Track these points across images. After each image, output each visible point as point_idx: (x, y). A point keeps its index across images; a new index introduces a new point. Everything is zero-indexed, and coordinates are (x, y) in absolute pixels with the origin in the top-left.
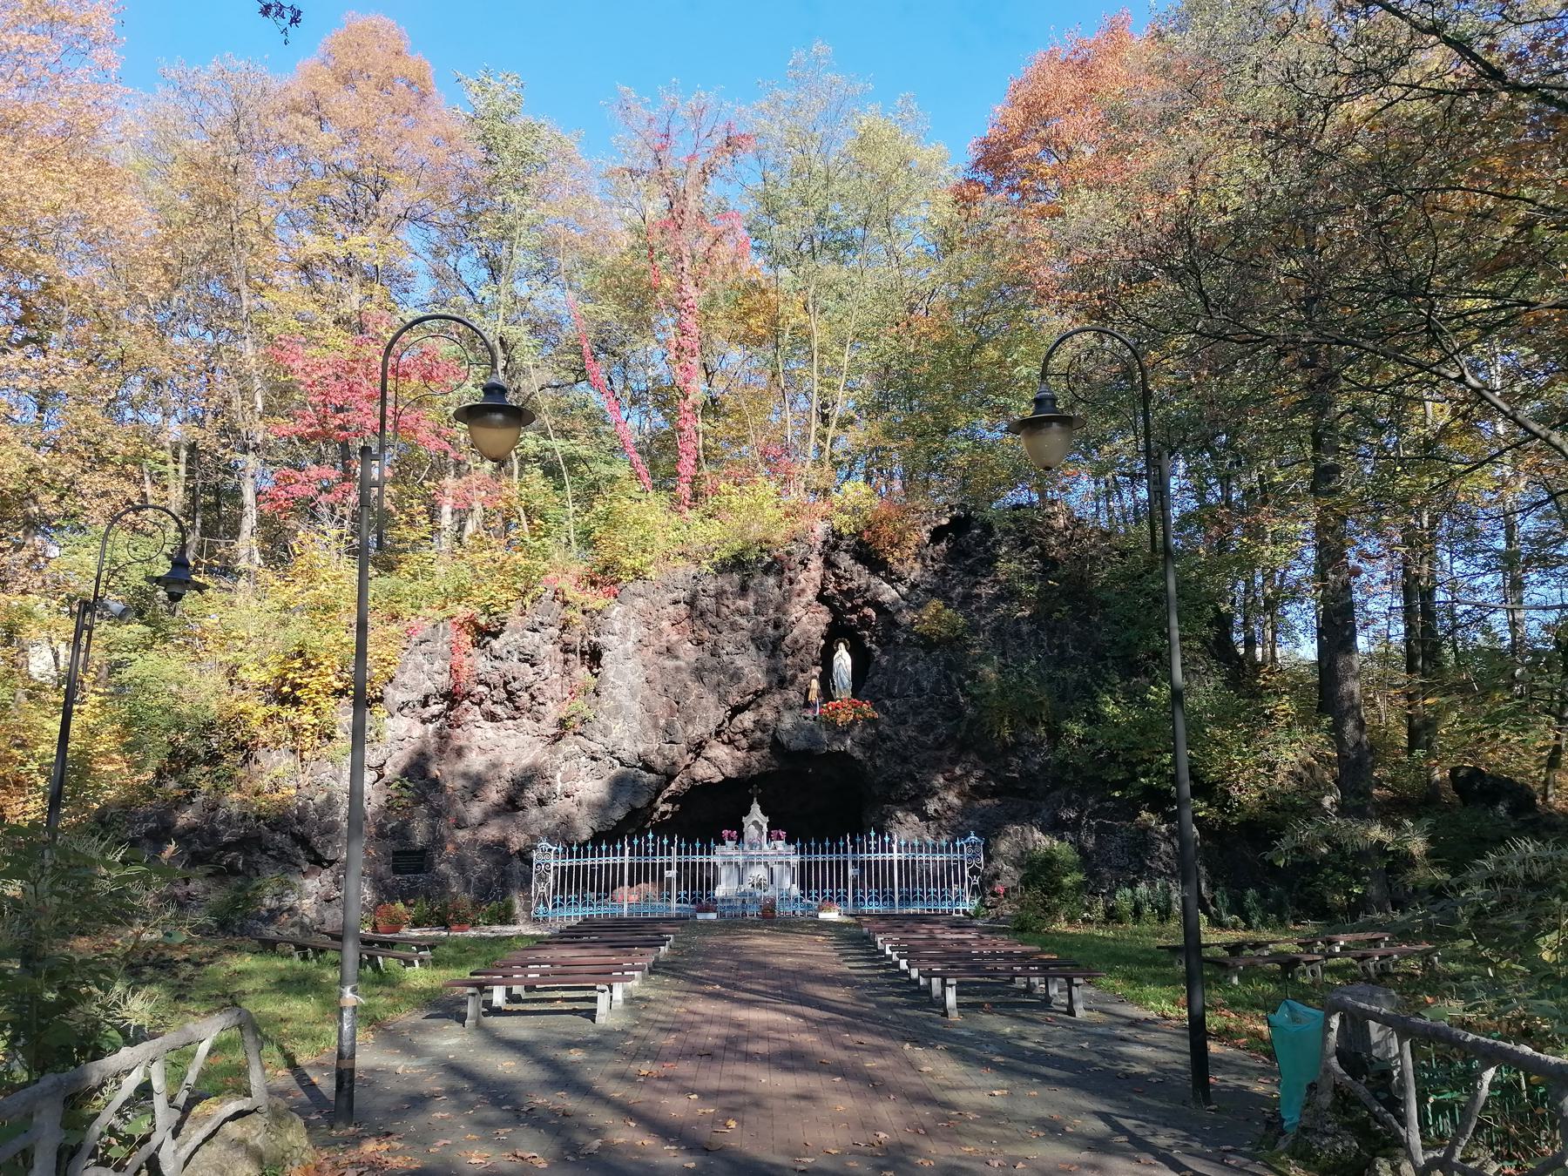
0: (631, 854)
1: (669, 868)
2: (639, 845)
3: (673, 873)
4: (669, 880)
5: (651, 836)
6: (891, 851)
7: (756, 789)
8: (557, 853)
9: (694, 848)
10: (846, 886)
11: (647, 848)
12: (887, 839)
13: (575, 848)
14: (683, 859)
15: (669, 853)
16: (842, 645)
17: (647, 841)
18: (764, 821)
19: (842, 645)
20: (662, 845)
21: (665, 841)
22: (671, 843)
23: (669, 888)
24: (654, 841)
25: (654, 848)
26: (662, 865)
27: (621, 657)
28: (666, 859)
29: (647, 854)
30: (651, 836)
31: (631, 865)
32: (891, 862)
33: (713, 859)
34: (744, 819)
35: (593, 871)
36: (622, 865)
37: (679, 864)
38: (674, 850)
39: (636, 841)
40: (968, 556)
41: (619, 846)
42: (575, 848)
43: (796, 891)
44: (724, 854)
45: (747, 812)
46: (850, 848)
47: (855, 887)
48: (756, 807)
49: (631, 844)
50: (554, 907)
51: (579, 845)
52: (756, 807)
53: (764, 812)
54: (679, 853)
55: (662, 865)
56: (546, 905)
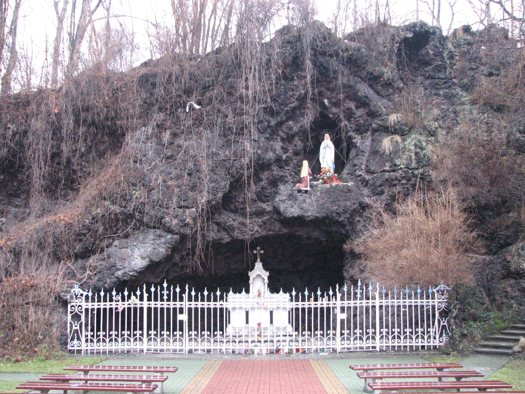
0: (149, 299)
1: (181, 311)
2: (156, 292)
3: (183, 317)
4: (181, 322)
5: (165, 285)
6: (374, 298)
7: (258, 251)
8: (87, 297)
9: (203, 296)
10: (335, 329)
11: (162, 295)
12: (370, 288)
13: (102, 294)
14: (193, 304)
15: (181, 299)
16: (327, 136)
17: (162, 289)
18: (266, 275)
19: (327, 136)
20: (175, 293)
21: (178, 290)
22: (183, 291)
23: (181, 330)
24: (168, 289)
25: (169, 295)
26: (175, 309)
27: (143, 138)
28: (178, 304)
29: (162, 300)
30: (165, 285)
31: (149, 309)
32: (374, 307)
33: (225, 305)
34: (250, 273)
35: (117, 314)
36: (142, 309)
37: (190, 309)
38: (186, 296)
39: (153, 289)
40: (427, 63)
41: (138, 293)
42: (102, 294)
43: (290, 329)
44: (234, 301)
45: (253, 268)
46: (339, 295)
47: (342, 328)
48: (259, 265)
49: (149, 291)
50: (87, 341)
51: (106, 291)
52: (259, 265)
53: (266, 268)
54: (190, 299)
55: (175, 309)
56: (79, 339)
